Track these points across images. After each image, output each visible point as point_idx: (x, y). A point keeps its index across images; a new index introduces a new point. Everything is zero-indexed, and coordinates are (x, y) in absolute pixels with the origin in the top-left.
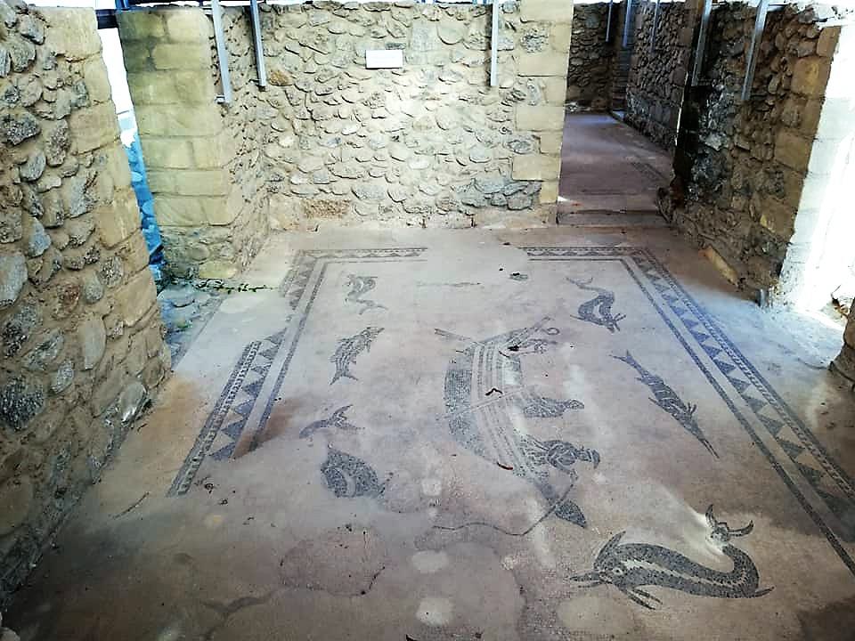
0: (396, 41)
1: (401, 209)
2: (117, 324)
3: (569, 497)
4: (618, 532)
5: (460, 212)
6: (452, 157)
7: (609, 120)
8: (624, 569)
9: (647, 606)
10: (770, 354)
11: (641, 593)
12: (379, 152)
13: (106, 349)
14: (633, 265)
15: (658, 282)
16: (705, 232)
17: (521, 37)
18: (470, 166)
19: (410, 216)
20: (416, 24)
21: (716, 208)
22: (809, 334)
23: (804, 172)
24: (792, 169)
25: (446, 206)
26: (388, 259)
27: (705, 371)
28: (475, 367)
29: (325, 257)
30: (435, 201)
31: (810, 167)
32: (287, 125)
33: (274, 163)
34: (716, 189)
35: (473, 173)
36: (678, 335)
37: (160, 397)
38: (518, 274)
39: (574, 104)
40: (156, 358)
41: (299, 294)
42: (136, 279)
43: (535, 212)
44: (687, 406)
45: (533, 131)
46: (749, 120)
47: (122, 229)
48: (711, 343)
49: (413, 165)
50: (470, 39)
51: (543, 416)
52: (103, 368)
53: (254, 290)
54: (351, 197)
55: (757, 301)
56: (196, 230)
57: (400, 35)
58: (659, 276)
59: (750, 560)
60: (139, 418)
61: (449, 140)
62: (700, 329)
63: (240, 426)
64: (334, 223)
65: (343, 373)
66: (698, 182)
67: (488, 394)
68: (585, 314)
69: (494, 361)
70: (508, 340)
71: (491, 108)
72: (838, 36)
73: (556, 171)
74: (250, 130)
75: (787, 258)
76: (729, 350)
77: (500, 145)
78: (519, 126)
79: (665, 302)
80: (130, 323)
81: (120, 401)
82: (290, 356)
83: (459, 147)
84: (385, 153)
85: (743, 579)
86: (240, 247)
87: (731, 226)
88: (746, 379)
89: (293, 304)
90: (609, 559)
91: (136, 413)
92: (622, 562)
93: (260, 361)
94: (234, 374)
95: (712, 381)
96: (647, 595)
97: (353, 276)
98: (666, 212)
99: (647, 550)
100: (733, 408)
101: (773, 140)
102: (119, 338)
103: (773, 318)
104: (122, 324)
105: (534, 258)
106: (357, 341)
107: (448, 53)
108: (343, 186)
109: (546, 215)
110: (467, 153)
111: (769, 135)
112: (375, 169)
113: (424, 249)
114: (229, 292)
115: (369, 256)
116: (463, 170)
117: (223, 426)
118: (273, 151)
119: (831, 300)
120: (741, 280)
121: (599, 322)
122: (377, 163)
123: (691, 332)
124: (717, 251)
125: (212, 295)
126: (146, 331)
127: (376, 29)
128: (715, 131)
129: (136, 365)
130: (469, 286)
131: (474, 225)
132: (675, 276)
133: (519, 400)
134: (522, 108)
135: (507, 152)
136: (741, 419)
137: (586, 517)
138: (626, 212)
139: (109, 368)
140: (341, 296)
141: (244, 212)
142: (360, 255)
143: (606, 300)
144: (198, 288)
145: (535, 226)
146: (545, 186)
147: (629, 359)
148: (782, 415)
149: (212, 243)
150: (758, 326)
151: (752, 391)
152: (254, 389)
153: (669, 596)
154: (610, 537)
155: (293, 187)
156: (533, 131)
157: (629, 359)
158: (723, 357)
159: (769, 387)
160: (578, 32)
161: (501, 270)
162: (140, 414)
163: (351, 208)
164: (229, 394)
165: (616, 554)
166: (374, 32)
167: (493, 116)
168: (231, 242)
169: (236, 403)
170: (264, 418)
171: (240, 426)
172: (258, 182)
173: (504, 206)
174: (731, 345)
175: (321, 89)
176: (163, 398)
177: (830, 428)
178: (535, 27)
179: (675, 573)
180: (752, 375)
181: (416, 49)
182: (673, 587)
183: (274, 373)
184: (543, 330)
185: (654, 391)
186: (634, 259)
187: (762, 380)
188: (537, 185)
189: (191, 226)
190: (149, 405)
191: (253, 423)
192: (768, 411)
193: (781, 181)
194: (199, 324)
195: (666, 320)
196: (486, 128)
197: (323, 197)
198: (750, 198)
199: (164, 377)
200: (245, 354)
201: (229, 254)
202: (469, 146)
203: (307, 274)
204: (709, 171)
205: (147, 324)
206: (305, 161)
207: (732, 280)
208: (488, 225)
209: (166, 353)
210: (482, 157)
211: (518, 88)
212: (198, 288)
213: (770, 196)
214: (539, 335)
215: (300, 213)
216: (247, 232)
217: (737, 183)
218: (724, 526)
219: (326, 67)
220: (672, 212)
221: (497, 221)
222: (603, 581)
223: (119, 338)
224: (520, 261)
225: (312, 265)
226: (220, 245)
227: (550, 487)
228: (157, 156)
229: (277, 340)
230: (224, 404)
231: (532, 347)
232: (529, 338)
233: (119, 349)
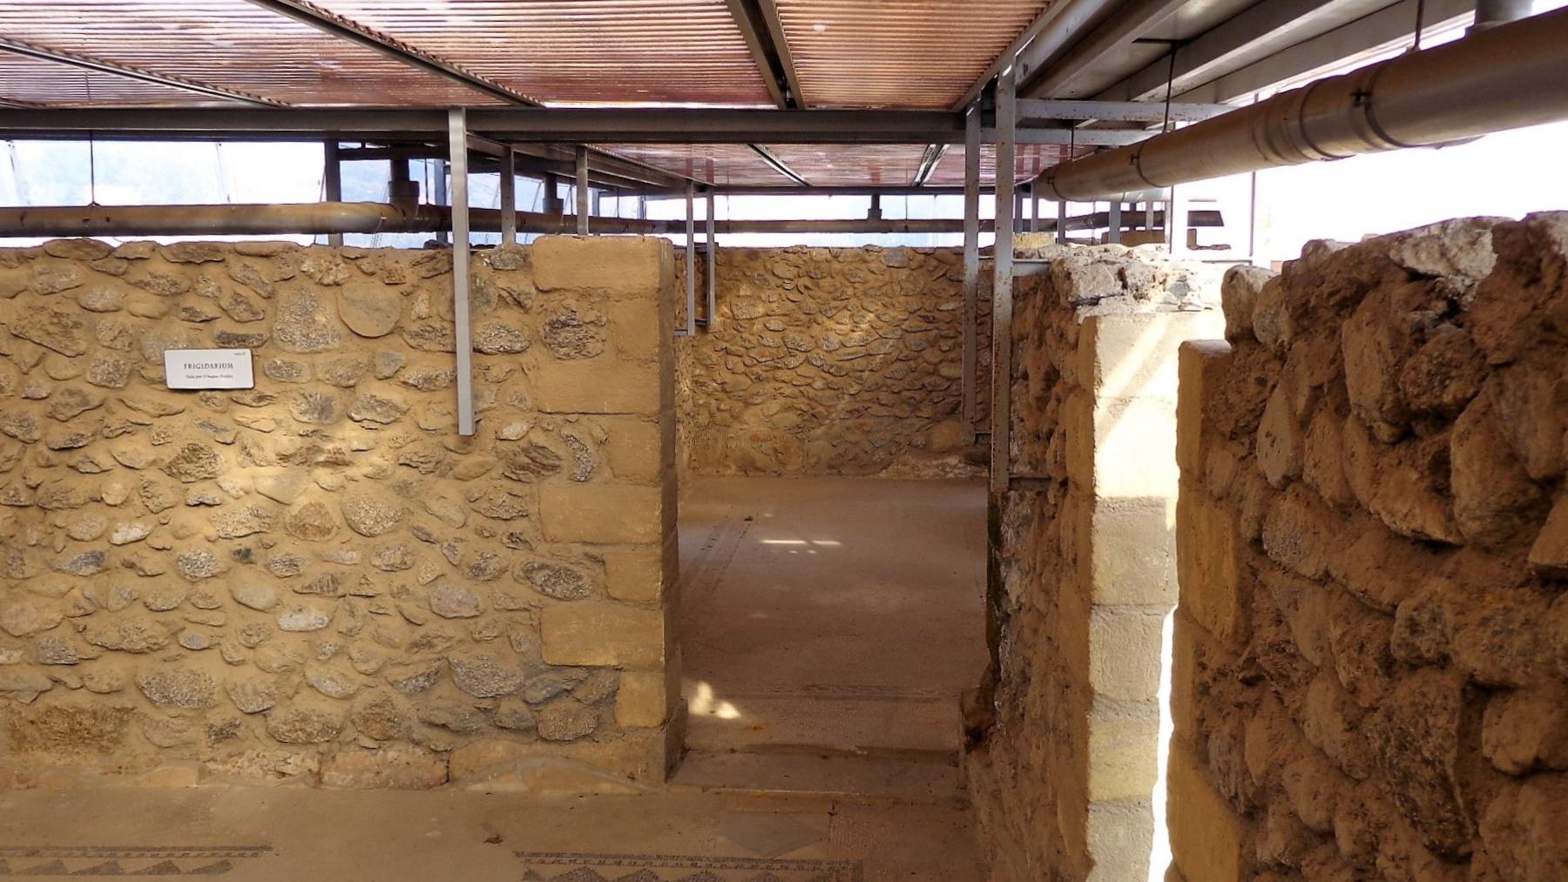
0: (241, 330)
1: (260, 732)
5: (417, 744)
6: (388, 603)
12: (201, 587)
17: (540, 324)
18: (433, 627)
19: (282, 753)
20: (284, 292)
31: (1099, 677)
35: (440, 645)
39: (953, 460)
43: (609, 750)
45: (585, 543)
49: (288, 621)
50: (415, 327)
57: (246, 316)
61: (377, 562)
64: (90, 763)
71: (476, 487)
72: (1095, 342)
77: (508, 574)
78: (551, 530)
83: (399, 579)
84: (218, 589)
107: (364, 360)
108: (110, 670)
110: (422, 592)
112: (191, 631)
122: (200, 616)
127: (191, 301)
134: (554, 493)
135: (525, 594)
138: (872, 754)
145: (605, 787)
146: (630, 682)
156: (585, 543)
160: (951, 306)
166: (185, 310)
167: (483, 505)
173: (527, 731)
175: (59, 435)
178: (571, 302)
181: (289, 347)
188: (606, 681)
196: (472, 536)
197: (61, 699)
206: (15, 607)
208: (481, 780)
210: (460, 603)
211: (538, 438)
219: (72, 385)
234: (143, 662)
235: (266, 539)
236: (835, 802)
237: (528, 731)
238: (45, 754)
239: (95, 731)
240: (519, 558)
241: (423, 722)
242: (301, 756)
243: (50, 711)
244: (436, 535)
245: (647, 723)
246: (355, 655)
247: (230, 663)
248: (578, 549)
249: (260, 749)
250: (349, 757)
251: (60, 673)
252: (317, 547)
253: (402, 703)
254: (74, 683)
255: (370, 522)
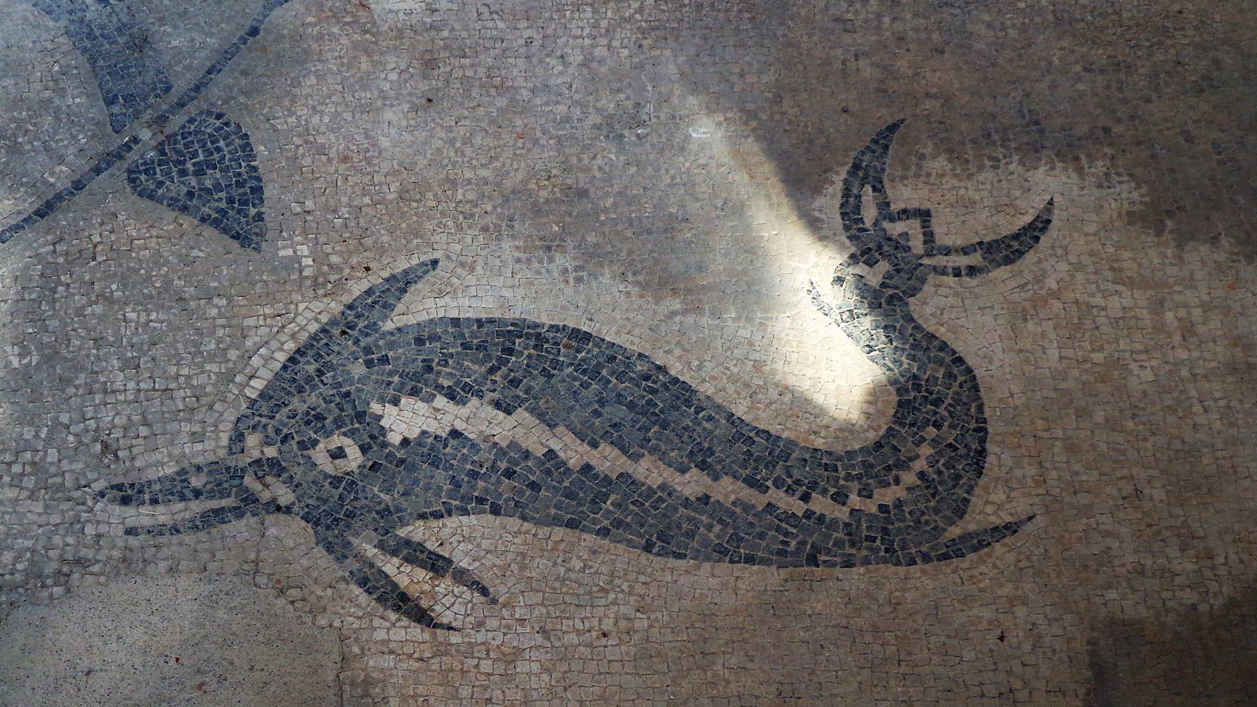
3: (215, 93)
4: (402, 265)
8: (373, 439)
9: (422, 617)
11: (414, 554)
59: (976, 388)
85: (909, 478)
90: (313, 399)
92: (376, 407)
96: (437, 565)
99: (510, 351)
137: (270, 191)
153: (540, 565)
154: (357, 289)
165: (358, 369)
179: (608, 460)
182: (571, 524)
218: (913, 227)
222: (249, 499)
227: (141, 43)
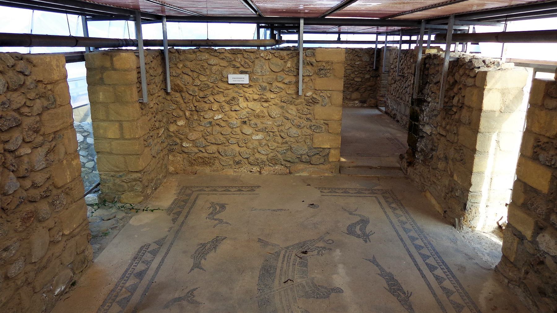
0: (246, 70)
1: (247, 162)
2: (58, 234)
5: (282, 165)
6: (277, 133)
7: (376, 112)
10: (460, 259)
12: (234, 129)
13: (48, 250)
14: (382, 201)
15: (396, 212)
16: (425, 182)
17: (316, 69)
18: (288, 139)
20: (257, 61)
21: (430, 167)
22: (484, 248)
23: (474, 151)
24: (468, 148)
25: (274, 161)
26: (235, 193)
27: (419, 270)
28: (279, 265)
29: (198, 191)
30: (267, 158)
31: (478, 147)
32: (181, 113)
33: (173, 135)
34: (430, 157)
36: (405, 245)
37: (82, 279)
38: (313, 204)
39: (357, 102)
40: (83, 254)
41: (179, 213)
42: (74, 206)
43: (327, 166)
44: (406, 293)
45: (324, 120)
46: (444, 119)
47: (68, 176)
48: (425, 251)
49: (254, 137)
50: (287, 70)
51: (317, 298)
52: (45, 260)
53: (152, 211)
54: (217, 155)
55: (454, 226)
56: (121, 174)
57: (247, 67)
58: (398, 208)
60: (66, 293)
61: (275, 124)
62: (419, 242)
63: (128, 300)
65: (197, 266)
66: (421, 152)
67: (285, 282)
68: (350, 231)
69: (292, 260)
70: (302, 247)
71: (299, 107)
72: (486, 77)
73: (338, 142)
74: (159, 117)
75: (469, 200)
76: (435, 256)
77: (305, 127)
78: (316, 117)
79: (399, 224)
80: (67, 232)
81: (54, 282)
82: (167, 253)
83: (280, 128)
84: (238, 130)
86: (146, 184)
87: (438, 179)
88: (445, 277)
89: (174, 220)
91: (65, 289)
93: (148, 257)
94: (131, 264)
95: (424, 276)
97: (213, 203)
98: (404, 168)
100: (435, 295)
101: (457, 131)
102: (58, 242)
103: (463, 236)
104: (61, 234)
105: (324, 194)
106: (209, 245)
107: (275, 77)
108: (214, 148)
109: (333, 168)
111: (455, 128)
112: (232, 139)
113: (259, 187)
114: (137, 212)
115: (224, 191)
116: (284, 141)
117: (118, 299)
118: (173, 128)
119: (497, 225)
120: (445, 212)
121: (358, 236)
123: (413, 244)
124: (431, 194)
125: (126, 213)
126: (77, 237)
127: (234, 63)
128: (428, 124)
129: (68, 258)
130: (283, 211)
131: (290, 173)
132: (406, 208)
133: (304, 287)
134: (318, 109)
135: (309, 132)
136: (439, 302)
138: (381, 168)
139: (49, 261)
140: (204, 215)
141: (151, 164)
142: (220, 189)
143: (364, 222)
144: (119, 208)
145: (327, 175)
146: (332, 151)
147: (374, 261)
148: (464, 300)
149: (130, 182)
150: (455, 241)
151: (447, 284)
152: (140, 275)
155: (183, 149)
157: (374, 261)
158: (431, 261)
159: (457, 281)
160: (358, 63)
161: (303, 201)
162: (67, 290)
163: (217, 161)
164: (125, 278)
166: (233, 65)
167: (301, 111)
168: (141, 182)
169: (128, 284)
170: (144, 294)
171: (128, 300)
172: (162, 145)
173: (308, 162)
174: (437, 253)
175: (202, 94)
176: (83, 280)
177: (493, 310)
178: (324, 64)
180: (448, 273)
181: (257, 74)
183: (154, 265)
184: (324, 241)
185: (387, 282)
186: (383, 196)
187: (454, 276)
188: (327, 151)
189: (118, 172)
190: (74, 284)
191: (136, 298)
192: (456, 297)
193: (462, 154)
194: (115, 232)
195: (399, 236)
197: (201, 155)
198: (447, 163)
199: (87, 266)
200: (139, 252)
201: (139, 189)
202: (287, 128)
203: (186, 202)
204: (426, 146)
205: (79, 233)
207: (440, 211)
208: (298, 173)
209: (89, 252)
211: (315, 96)
212: (119, 208)
213: (458, 163)
214: (321, 244)
215: (186, 163)
216: (153, 175)
217: (440, 154)
219: (205, 82)
220: (407, 168)
221: (304, 171)
223: (58, 242)
224: (315, 195)
225: (189, 195)
226: (134, 183)
228: (101, 131)
229: (160, 243)
230: (121, 285)
231: (316, 252)
232: (316, 245)
233: (57, 249)
234: (220, 146)
235: (250, 119)
236: (378, 177)
237: (310, 163)
238: (197, 167)
239: (208, 162)
240: (309, 123)
241: (284, 160)
242: (256, 167)
243: (198, 157)
244: (290, 118)
245: (335, 160)
246: (270, 145)
247: (240, 147)
248: (322, 122)
249: (246, 166)
250: (267, 168)
251: (201, 149)
252: (262, 121)
253: (280, 156)
254: (204, 151)
255: (274, 115)
